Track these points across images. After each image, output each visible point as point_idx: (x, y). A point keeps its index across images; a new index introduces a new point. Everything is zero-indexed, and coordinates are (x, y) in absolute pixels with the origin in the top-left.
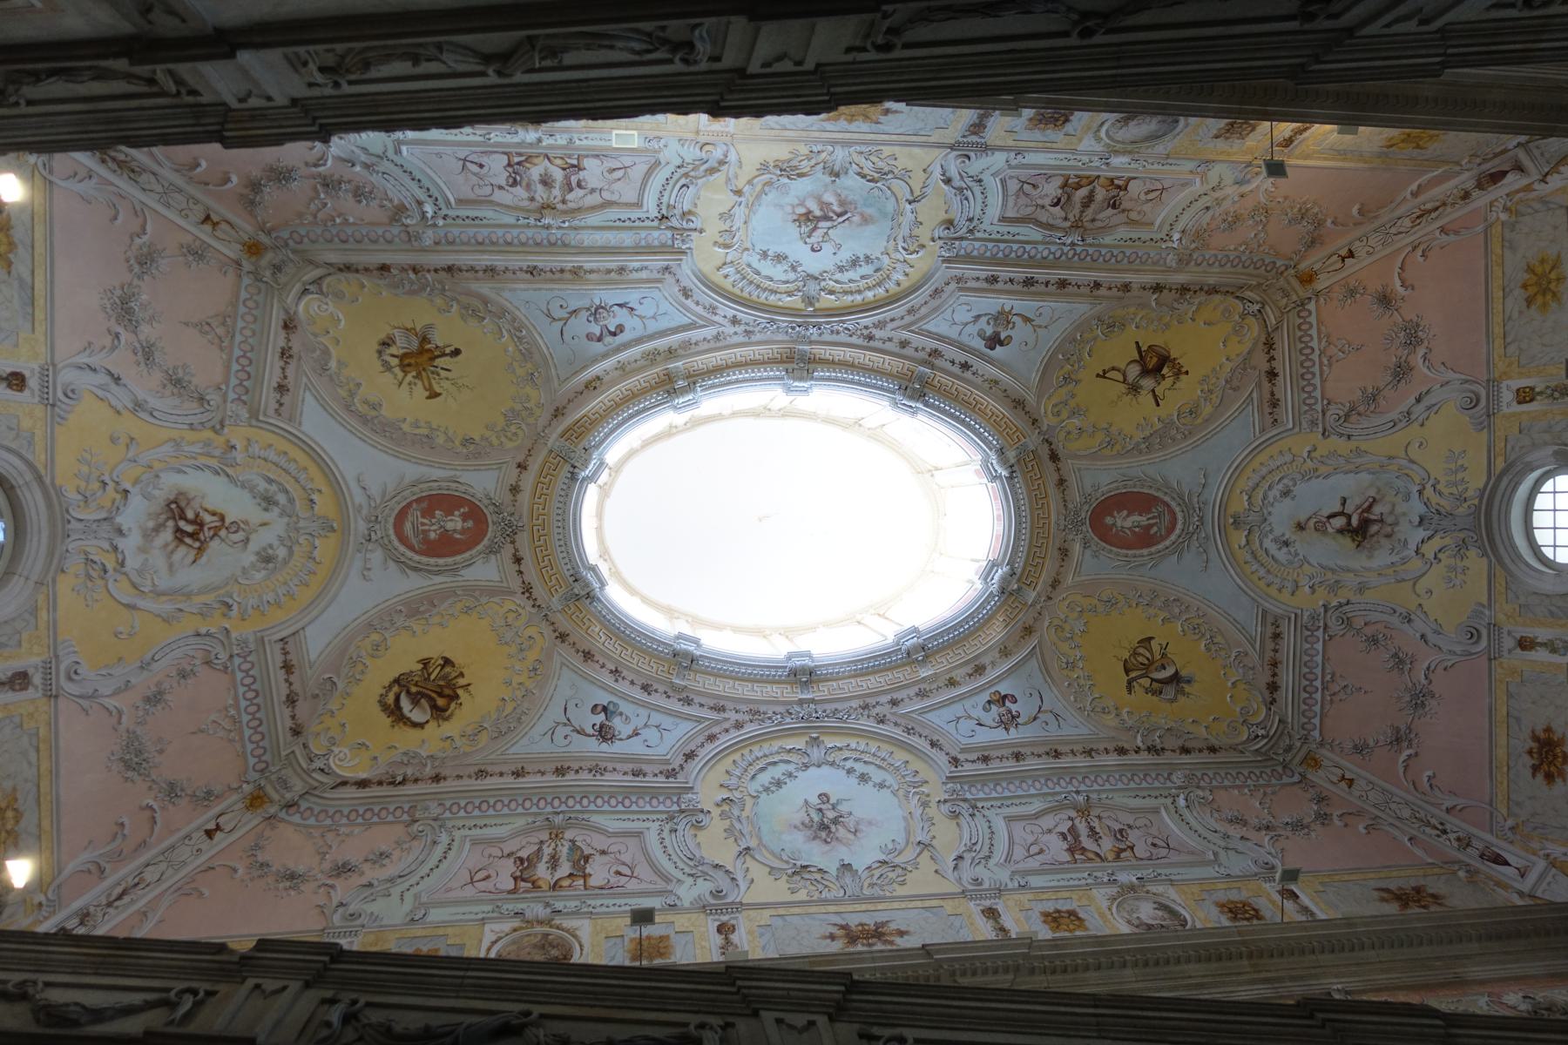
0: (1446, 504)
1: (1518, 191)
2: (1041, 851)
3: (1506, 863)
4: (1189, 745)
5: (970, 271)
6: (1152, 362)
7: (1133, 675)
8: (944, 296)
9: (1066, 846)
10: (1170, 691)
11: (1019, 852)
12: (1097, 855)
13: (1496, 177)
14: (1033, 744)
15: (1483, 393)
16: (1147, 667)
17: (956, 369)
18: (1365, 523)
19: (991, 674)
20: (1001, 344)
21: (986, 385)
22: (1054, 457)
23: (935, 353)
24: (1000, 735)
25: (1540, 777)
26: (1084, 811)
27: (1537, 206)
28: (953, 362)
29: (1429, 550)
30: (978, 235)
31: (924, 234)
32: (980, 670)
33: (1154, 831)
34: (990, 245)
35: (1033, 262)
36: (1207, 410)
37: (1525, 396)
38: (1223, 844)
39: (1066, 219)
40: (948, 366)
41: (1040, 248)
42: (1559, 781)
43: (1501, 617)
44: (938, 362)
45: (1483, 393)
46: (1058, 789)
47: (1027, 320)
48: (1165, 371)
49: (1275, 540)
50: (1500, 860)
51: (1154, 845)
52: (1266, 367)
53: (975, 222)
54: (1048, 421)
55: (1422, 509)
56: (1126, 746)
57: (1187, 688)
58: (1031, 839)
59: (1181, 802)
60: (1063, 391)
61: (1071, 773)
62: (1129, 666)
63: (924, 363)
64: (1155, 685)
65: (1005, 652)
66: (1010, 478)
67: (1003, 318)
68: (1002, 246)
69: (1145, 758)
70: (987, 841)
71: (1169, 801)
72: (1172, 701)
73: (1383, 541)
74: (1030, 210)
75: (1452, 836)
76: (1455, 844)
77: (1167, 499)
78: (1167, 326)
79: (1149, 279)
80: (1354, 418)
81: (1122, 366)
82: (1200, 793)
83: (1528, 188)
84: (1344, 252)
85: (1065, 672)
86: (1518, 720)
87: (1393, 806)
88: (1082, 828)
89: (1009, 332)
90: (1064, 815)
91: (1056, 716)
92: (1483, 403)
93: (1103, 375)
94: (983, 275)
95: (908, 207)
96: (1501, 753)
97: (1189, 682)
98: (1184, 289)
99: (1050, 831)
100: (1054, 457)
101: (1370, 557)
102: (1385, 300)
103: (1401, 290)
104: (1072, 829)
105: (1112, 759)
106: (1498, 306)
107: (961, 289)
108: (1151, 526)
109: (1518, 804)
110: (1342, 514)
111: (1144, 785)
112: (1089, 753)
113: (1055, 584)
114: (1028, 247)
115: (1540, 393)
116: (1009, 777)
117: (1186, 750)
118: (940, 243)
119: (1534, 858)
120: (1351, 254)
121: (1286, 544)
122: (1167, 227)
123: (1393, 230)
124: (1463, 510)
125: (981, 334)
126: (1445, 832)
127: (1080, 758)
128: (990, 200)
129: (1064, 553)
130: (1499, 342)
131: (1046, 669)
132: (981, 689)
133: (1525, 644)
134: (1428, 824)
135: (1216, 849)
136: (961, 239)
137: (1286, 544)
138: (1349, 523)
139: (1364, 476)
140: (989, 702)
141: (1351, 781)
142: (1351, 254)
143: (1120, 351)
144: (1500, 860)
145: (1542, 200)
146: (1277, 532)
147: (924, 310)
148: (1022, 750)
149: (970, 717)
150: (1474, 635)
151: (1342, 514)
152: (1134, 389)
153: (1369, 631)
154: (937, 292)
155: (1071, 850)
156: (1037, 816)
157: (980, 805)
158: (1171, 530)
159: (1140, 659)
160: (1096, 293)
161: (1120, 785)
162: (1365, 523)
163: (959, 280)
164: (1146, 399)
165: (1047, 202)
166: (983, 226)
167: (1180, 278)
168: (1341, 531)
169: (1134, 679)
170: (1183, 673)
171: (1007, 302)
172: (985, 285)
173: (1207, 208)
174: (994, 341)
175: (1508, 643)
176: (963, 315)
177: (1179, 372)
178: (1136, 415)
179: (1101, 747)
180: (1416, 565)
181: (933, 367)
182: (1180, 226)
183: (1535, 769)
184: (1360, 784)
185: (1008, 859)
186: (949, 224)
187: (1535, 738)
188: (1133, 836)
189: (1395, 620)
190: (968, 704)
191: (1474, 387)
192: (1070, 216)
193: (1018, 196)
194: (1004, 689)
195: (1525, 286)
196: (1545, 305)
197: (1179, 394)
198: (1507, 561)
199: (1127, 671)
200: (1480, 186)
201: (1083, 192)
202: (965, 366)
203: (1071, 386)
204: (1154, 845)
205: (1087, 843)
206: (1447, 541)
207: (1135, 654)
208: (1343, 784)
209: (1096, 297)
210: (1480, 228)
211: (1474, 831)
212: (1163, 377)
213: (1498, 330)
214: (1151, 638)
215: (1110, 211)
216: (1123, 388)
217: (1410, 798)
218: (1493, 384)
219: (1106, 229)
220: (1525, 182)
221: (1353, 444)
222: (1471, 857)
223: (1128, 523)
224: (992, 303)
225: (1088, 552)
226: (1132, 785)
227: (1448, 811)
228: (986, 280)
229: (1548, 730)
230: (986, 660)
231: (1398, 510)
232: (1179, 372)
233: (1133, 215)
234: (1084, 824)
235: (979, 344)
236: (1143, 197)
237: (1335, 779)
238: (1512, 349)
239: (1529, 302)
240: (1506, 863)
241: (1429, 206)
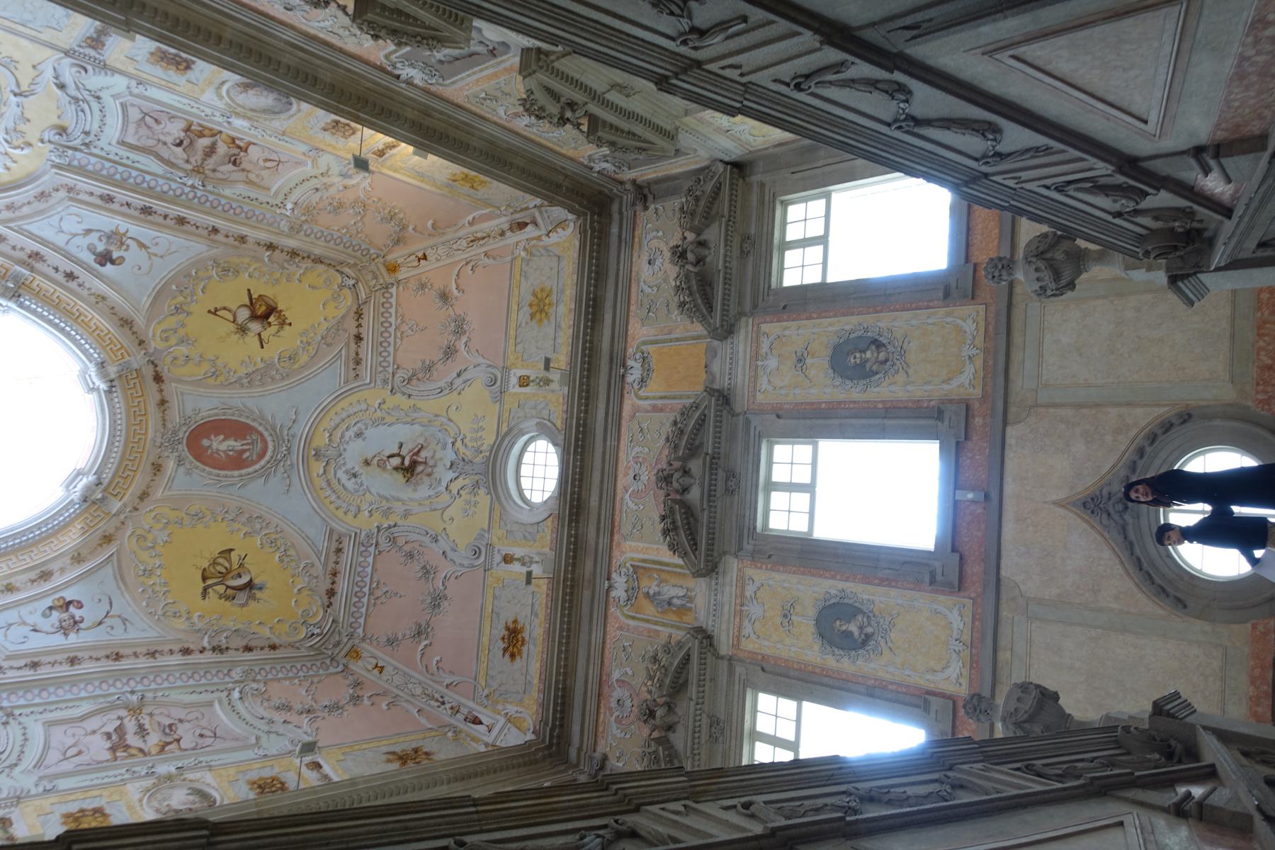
0: (469, 454)
1: (532, 239)
2: (80, 753)
3: (481, 723)
4: (252, 644)
5: (83, 184)
6: (261, 310)
7: (210, 582)
8: (52, 201)
9: (108, 745)
10: (242, 597)
11: (53, 756)
12: (141, 750)
13: (522, 225)
14: (94, 648)
15: (499, 375)
16: (223, 576)
17: (60, 277)
18: (414, 464)
19: (57, 580)
20: (113, 262)
21: (93, 299)
22: (158, 378)
23: (36, 256)
24: (58, 640)
25: (507, 655)
26: (135, 710)
27: (543, 252)
28: (56, 269)
29: (455, 487)
30: (94, 151)
31: (32, 133)
32: (46, 576)
33: (204, 723)
34: (107, 164)
35: (150, 192)
36: (304, 358)
37: (524, 382)
38: (266, 728)
39: (187, 161)
40: (51, 272)
41: (161, 181)
42: (518, 658)
43: (495, 539)
44: (38, 265)
45: (499, 375)
46: (112, 690)
47: (142, 245)
48: (271, 319)
49: (347, 472)
50: (476, 721)
51: (201, 736)
52: (354, 331)
53: (91, 138)
54: (155, 344)
55: (452, 456)
56: (192, 647)
57: (258, 594)
58: (70, 741)
59: (236, 694)
60: (174, 319)
61: (129, 674)
62: (207, 574)
63: (22, 263)
64: (230, 592)
65: (78, 559)
66: (109, 392)
67: (116, 237)
68: (121, 169)
69: (209, 657)
70: (17, 749)
71: (225, 693)
72: (243, 606)
73: (425, 479)
74: (151, 142)
75: (448, 706)
76: (449, 712)
77: (261, 429)
78: (277, 281)
79: (264, 236)
80: (414, 382)
81: (234, 308)
82: (255, 685)
83: (539, 238)
84: (420, 255)
85: (141, 579)
86: (498, 615)
87: (410, 686)
88: (131, 726)
89: (122, 253)
90: (113, 715)
91: (124, 621)
92: (498, 383)
93: (214, 312)
94: (98, 191)
95: (12, 98)
96: (485, 640)
97: (261, 589)
98: (294, 254)
99: (94, 732)
100: (158, 378)
101: (415, 490)
102: (444, 297)
103: (455, 292)
104: (120, 730)
105: (177, 659)
106: (514, 316)
107: (71, 199)
108: (245, 451)
109: (492, 677)
110: (398, 455)
111: (203, 681)
112: (152, 654)
113: (144, 496)
114: (148, 178)
116: (58, 682)
117: (248, 649)
118: (52, 147)
119: (498, 717)
120: (425, 258)
121: (355, 476)
122: (281, 197)
123: (455, 247)
124: (479, 459)
125: (91, 249)
126: (443, 703)
127: (142, 659)
128: (108, 120)
129: (157, 468)
130: (512, 341)
131: (121, 576)
132: (43, 595)
133: (508, 559)
134: (433, 698)
135: (259, 733)
136: (75, 149)
137: (355, 476)
138: (403, 463)
139: (416, 427)
140: (51, 608)
141: (382, 668)
142: (425, 258)
143: (233, 294)
144: (476, 721)
145: (545, 248)
146: (349, 466)
147: (25, 210)
148: (80, 655)
149: (24, 623)
150: (477, 553)
151: (398, 455)
152: (243, 330)
153: (407, 548)
154: (42, 196)
155: (113, 749)
156: (83, 718)
157: (17, 712)
158: (261, 456)
159: (219, 568)
160: (213, 236)
161: (179, 683)
162: (414, 464)
163: (70, 190)
164: (252, 340)
165: (169, 140)
166: (100, 144)
167: (292, 243)
168: (396, 469)
169: (209, 586)
170: (256, 581)
171: (123, 225)
172: (99, 202)
173: (317, 190)
174: (105, 258)
175: (498, 558)
176: (71, 225)
177: (283, 323)
178: (242, 352)
179: (166, 648)
180: (445, 498)
181: (32, 269)
182: (293, 198)
183: (505, 650)
184: (388, 669)
185: (38, 765)
186: (62, 130)
187: (507, 628)
188: (181, 730)
189: (427, 540)
190: (24, 610)
191: (494, 371)
192: (192, 160)
193: (139, 126)
194: (69, 595)
195: (530, 305)
196: (540, 320)
197: (281, 341)
198: (503, 499)
199: (204, 579)
200: (511, 229)
201: (204, 142)
202: (70, 276)
203: (182, 316)
204: (201, 736)
205: (132, 740)
206: (467, 481)
207: (214, 563)
208: (376, 671)
209: (214, 241)
210: (509, 258)
211: (463, 700)
212: (270, 324)
213: (512, 333)
214: (231, 550)
215: (230, 167)
216: (232, 327)
217: (422, 678)
218: (506, 370)
219: (226, 181)
220: (537, 233)
221: (411, 402)
222: (458, 721)
223: (224, 446)
224: (107, 221)
225: (182, 469)
226: (191, 682)
227: (447, 686)
228: (101, 197)
229: (515, 621)
230: (54, 566)
231: (437, 456)
232: (283, 323)
233: (252, 177)
234: (134, 722)
235: (89, 258)
236: (261, 162)
237: (370, 667)
238: (520, 347)
239: (532, 316)
240: (481, 723)
241: (479, 235)
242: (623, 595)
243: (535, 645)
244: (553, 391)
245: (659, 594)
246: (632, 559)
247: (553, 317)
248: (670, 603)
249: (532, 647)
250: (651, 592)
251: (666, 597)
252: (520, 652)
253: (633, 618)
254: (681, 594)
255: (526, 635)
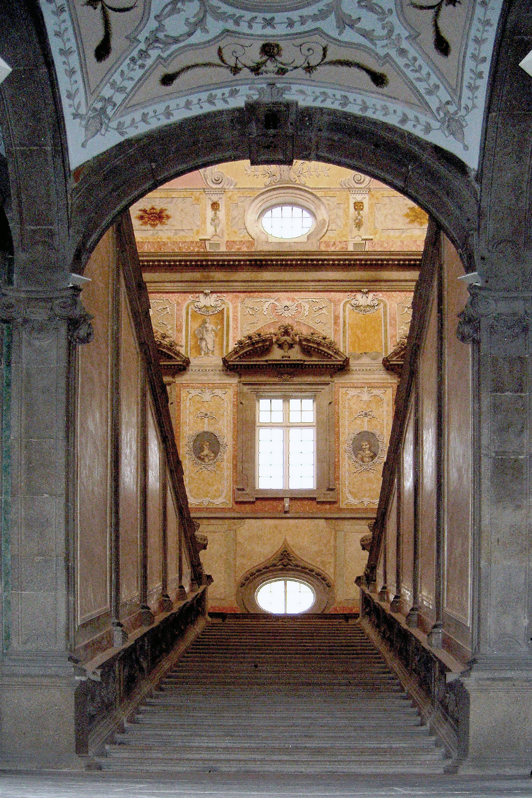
15: (362, 186)
25: (141, 213)
37: (358, 206)
42: (141, 222)
45: (362, 186)
86: (171, 202)
115: (359, 214)
133: (215, 206)
175: (215, 198)
183: (145, 211)
187: (162, 211)
196: (407, 215)
198: (262, 197)
229: (168, 217)
238: (387, 200)
242: (201, 304)
243: (153, 235)
244: (351, 231)
245: (207, 331)
246: (228, 309)
247: (411, 226)
248: (201, 339)
249: (151, 232)
250: (207, 325)
251: (205, 337)
252: (145, 223)
253: (187, 313)
254: (210, 346)
255: (159, 227)
